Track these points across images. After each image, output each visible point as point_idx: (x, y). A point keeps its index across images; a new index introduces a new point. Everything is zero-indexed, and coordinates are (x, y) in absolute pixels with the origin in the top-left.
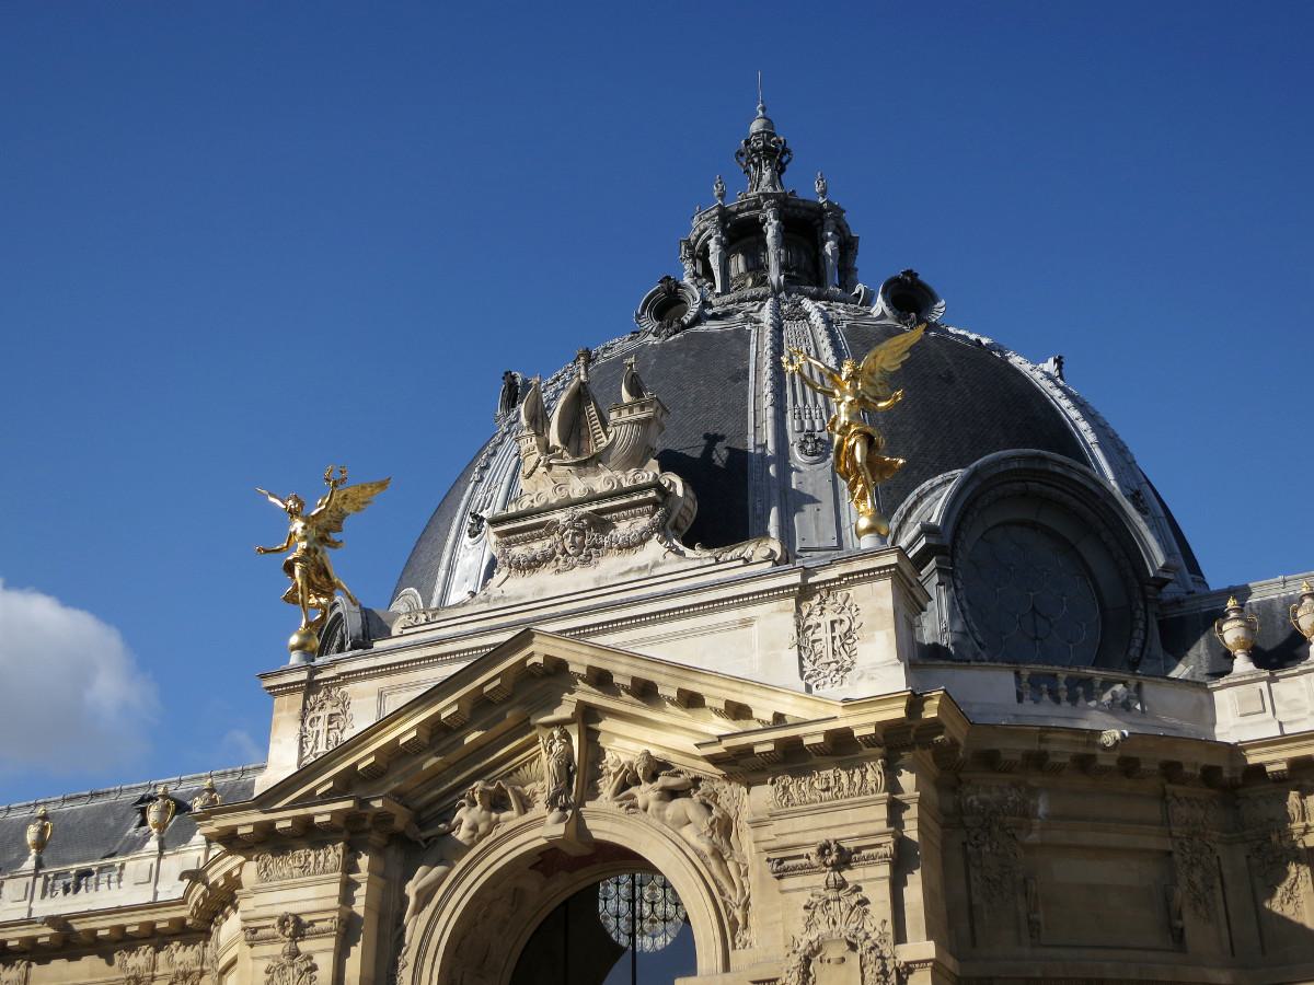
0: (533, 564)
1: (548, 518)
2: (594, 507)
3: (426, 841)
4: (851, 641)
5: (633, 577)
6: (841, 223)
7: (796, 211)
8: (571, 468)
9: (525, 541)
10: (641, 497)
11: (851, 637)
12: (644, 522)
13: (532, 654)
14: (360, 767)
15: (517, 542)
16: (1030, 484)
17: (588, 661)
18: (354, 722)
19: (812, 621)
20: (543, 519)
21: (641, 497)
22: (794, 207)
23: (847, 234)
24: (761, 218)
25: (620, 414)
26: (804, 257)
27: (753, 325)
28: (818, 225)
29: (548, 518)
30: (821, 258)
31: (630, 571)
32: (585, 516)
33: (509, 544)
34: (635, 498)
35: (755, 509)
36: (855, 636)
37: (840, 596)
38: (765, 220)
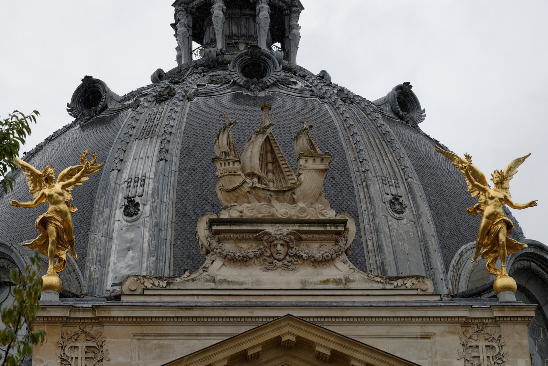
2: (297, 228)
4: (500, 362)
5: (331, 286)
8: (272, 194)
10: (333, 228)
11: (500, 359)
12: (329, 248)
13: (289, 333)
15: (231, 238)
16: (532, 263)
17: (333, 346)
18: (111, 356)
19: (474, 343)
21: (333, 228)
28: (287, 15)
31: (327, 282)
33: (219, 241)
34: (328, 228)
36: (504, 359)
37: (489, 329)
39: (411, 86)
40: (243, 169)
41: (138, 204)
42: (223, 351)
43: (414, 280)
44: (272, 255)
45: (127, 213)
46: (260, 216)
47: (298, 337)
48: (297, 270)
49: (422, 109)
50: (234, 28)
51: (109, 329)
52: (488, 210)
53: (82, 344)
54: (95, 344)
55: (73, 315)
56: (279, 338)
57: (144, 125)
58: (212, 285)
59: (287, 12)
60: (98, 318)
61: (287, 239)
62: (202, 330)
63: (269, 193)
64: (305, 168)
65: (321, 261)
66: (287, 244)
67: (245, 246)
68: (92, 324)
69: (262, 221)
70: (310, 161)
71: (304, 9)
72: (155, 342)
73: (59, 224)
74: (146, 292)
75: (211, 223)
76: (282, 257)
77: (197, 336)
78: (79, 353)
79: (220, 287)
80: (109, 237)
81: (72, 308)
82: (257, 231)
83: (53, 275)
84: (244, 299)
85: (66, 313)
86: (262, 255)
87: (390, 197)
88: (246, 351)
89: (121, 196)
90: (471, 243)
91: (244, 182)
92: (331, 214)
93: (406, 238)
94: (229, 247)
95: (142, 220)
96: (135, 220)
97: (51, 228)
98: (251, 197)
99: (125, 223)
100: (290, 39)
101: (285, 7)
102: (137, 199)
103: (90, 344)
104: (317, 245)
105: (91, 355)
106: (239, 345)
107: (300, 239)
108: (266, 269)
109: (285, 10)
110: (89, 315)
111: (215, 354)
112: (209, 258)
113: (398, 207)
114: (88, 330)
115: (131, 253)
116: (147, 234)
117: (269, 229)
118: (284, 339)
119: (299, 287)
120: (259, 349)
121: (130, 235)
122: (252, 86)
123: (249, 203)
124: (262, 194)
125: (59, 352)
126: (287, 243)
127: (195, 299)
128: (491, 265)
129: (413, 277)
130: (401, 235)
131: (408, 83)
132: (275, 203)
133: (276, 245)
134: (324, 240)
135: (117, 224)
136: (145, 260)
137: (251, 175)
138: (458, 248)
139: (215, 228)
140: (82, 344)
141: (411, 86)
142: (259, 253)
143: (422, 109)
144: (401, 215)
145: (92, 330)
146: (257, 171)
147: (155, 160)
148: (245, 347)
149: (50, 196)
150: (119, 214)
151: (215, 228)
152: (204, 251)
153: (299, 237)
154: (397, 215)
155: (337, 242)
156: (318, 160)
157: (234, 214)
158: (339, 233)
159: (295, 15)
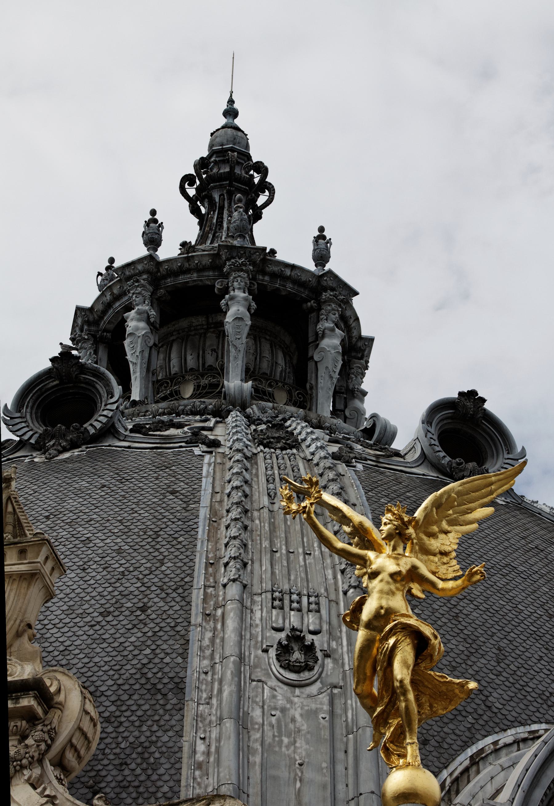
6: (348, 313)
22: (274, 276)
23: (355, 333)
24: (218, 286)
26: (281, 360)
27: (205, 448)
28: (312, 310)
30: (311, 365)
38: (226, 290)
39: (483, 400)
49: (519, 449)
50: (189, 358)
59: (309, 304)
71: (356, 293)
90: (521, 729)
100: (316, 363)
101: (305, 294)
109: (307, 301)
113: (297, 656)
122: (50, 441)
128: (391, 747)
130: (293, 720)
131: (473, 393)
138: (472, 741)
141: (483, 400)
143: (519, 449)
144: (305, 675)
154: (292, 676)
159: (329, 308)
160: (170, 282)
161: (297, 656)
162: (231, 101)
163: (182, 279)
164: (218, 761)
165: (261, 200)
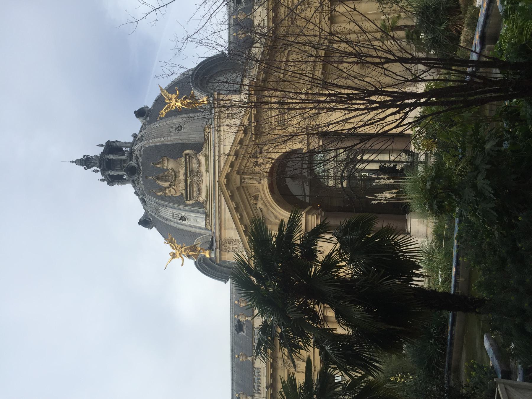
0: (200, 190)
1: (188, 184)
2: (188, 172)
3: (263, 218)
5: (208, 162)
7: (107, 151)
9: (193, 192)
12: (194, 160)
13: (224, 182)
14: (244, 229)
15: (193, 194)
17: (228, 167)
18: (232, 237)
20: (189, 186)
21: (188, 159)
25: (165, 166)
29: (188, 184)
32: (190, 174)
33: (193, 197)
34: (188, 161)
35: (193, 141)
38: (108, 159)
40: (168, 188)
41: (182, 217)
42: (230, 203)
43: (205, 132)
44: (198, 181)
45: (185, 220)
46: (184, 184)
47: (225, 178)
48: (202, 172)
51: (223, 237)
52: (180, 105)
53: (228, 245)
54: (228, 241)
55: (219, 248)
56: (225, 185)
57: (154, 210)
58: (208, 202)
60: (219, 240)
61: (192, 176)
62: (223, 207)
63: (176, 180)
64: (167, 167)
65: (199, 164)
66: (194, 176)
67: (195, 189)
68: (221, 242)
69: (186, 184)
70: (165, 165)
72: (227, 222)
73: (189, 251)
74: (211, 223)
75: (187, 200)
76: (198, 177)
77: (225, 209)
78: (231, 246)
79: (209, 199)
80: (193, 226)
81: (216, 248)
82: (190, 185)
83: (206, 253)
84: (213, 192)
85: (218, 250)
86: (198, 184)
87: (176, 130)
88: (230, 196)
89: (179, 221)
91: (173, 188)
92: (183, 159)
93: (191, 127)
94: (195, 194)
95: (186, 216)
96: (187, 218)
97: (190, 254)
98: (178, 186)
99: (188, 221)
102: (180, 217)
103: (228, 243)
104: (194, 165)
105: (231, 242)
106: (228, 198)
107: (192, 170)
108: (202, 183)
110: (218, 243)
111: (231, 206)
112: (199, 200)
113: (180, 128)
114: (223, 243)
115: (198, 220)
116: (191, 215)
117: (189, 181)
118: (226, 183)
119: (208, 173)
120: (229, 191)
121: (192, 220)
123: (180, 186)
124: (177, 182)
125: (230, 253)
126: (193, 175)
127: (213, 208)
129: (204, 132)
132: (180, 178)
133: (194, 179)
134: (192, 162)
135: (188, 223)
136: (200, 216)
137: (170, 185)
139: (189, 199)
140: (228, 245)
142: (197, 185)
145: (223, 242)
146: (169, 183)
147: (166, 209)
148: (228, 196)
149: (180, 254)
150: (185, 222)
151: (189, 199)
152: (197, 202)
153: (191, 172)
155: (193, 158)
156: (164, 162)
157: (184, 192)
158: (190, 157)
160: (105, 168)
161: (180, 128)
162: (70, 162)
163: (105, 166)
164: (195, 137)
165: (89, 157)
